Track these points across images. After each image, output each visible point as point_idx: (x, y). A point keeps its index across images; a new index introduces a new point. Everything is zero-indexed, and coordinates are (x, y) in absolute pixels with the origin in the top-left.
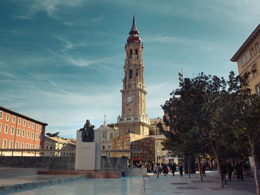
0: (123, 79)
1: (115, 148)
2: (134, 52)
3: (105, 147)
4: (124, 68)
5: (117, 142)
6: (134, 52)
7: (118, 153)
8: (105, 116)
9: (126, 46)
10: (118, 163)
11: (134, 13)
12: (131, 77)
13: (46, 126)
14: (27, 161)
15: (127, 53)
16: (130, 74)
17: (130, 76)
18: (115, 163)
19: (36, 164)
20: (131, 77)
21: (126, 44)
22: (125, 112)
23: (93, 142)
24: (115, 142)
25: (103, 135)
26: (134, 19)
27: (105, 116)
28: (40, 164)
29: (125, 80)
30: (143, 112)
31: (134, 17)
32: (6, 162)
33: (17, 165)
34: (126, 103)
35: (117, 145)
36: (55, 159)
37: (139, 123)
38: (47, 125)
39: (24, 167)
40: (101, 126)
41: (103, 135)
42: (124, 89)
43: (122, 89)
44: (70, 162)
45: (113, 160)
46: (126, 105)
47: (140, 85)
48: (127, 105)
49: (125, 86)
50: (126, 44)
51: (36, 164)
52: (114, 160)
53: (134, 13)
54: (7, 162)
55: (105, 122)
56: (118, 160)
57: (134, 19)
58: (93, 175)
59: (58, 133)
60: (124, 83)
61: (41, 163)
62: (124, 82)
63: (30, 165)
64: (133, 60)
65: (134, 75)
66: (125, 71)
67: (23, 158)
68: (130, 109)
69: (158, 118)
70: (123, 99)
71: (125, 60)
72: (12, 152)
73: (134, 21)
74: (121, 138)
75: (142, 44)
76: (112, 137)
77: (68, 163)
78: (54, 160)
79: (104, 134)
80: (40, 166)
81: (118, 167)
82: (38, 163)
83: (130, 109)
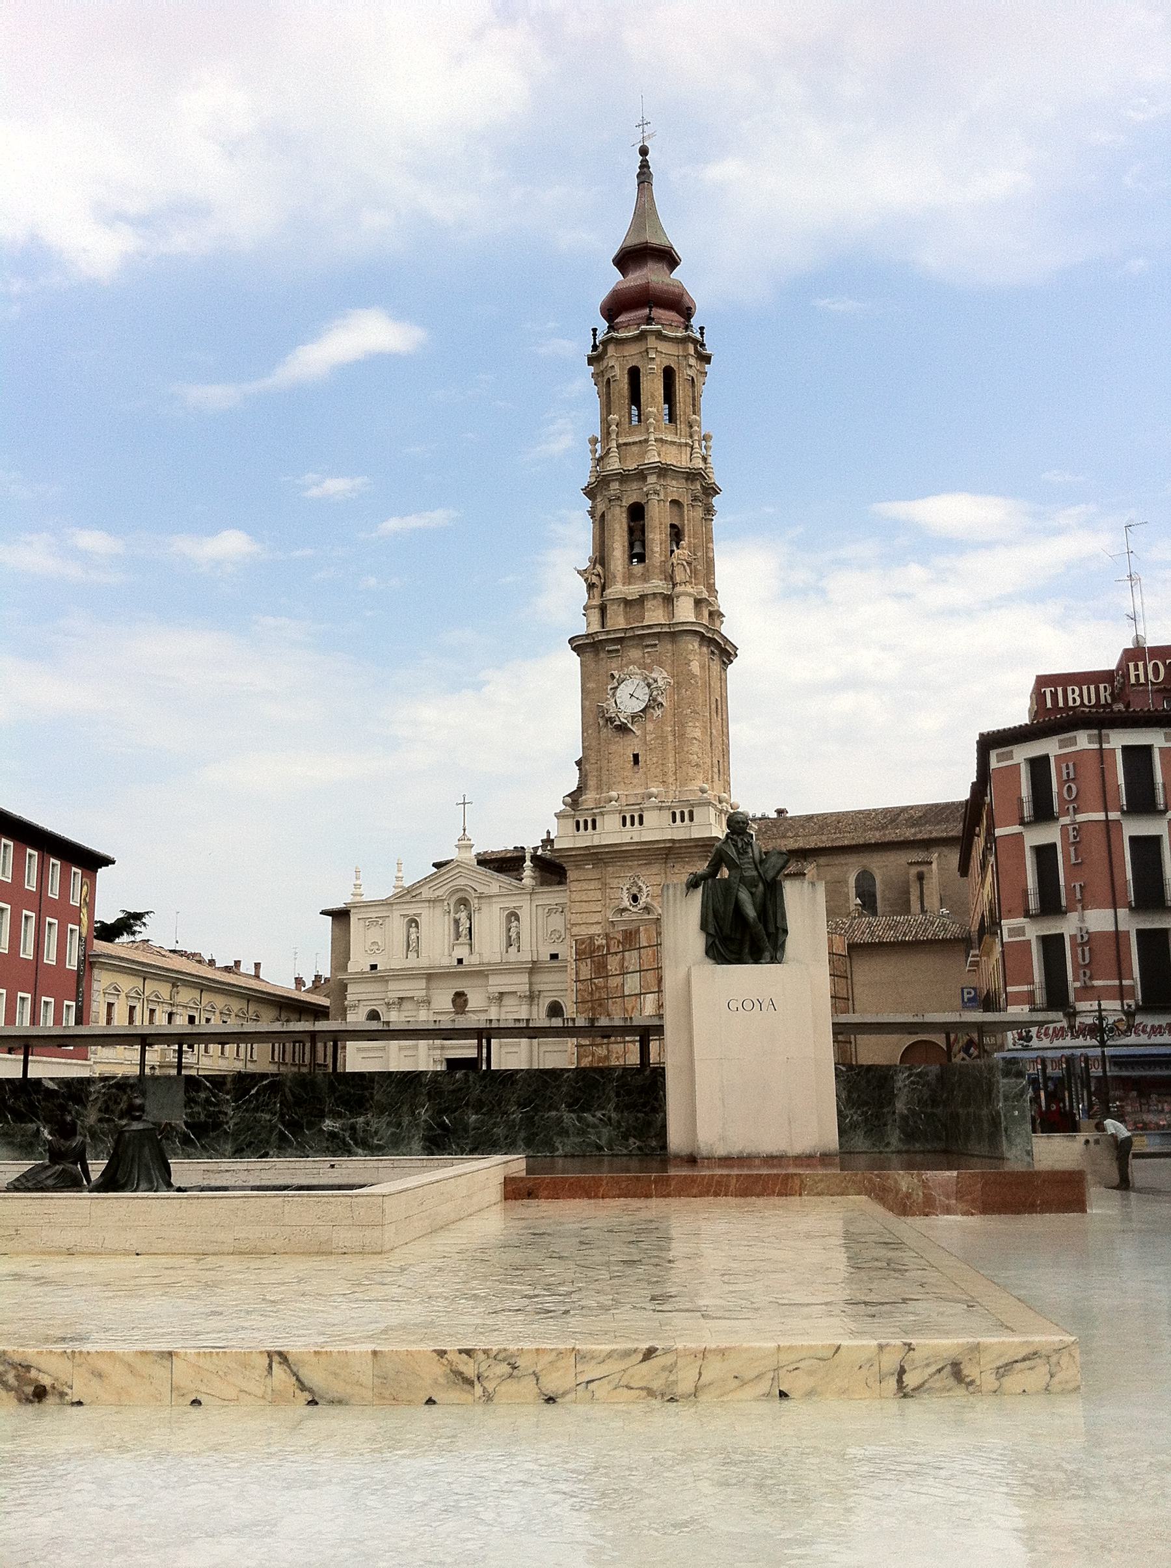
0: (586, 565)
1: (593, 1001)
2: (652, 386)
3: (466, 1001)
4: (590, 492)
5: (613, 964)
6: (652, 386)
7: (627, 1039)
8: (464, 804)
9: (595, 347)
10: (900, 1106)
11: (644, 124)
12: (637, 553)
13: (102, 872)
14: (256, 1109)
15: (608, 394)
16: (631, 531)
17: (631, 545)
18: (882, 1107)
19: (328, 1124)
20: (637, 553)
21: (595, 330)
22: (604, 778)
23: (775, 959)
24: (601, 968)
25: (457, 922)
26: (644, 165)
27: (464, 804)
28: (353, 1128)
29: (599, 568)
30: (716, 777)
31: (644, 151)
32: (100, 1120)
33: (186, 1141)
34: (610, 720)
35: (613, 982)
36: (460, 1089)
37: (702, 846)
38: (107, 861)
39: (238, 1152)
40: (436, 865)
41: (457, 922)
42: (596, 627)
43: (580, 627)
44: (569, 1106)
45: (863, 1082)
46: (607, 732)
47: (698, 602)
48: (623, 729)
49: (603, 609)
50: (595, 330)
51: (328, 1124)
52: (868, 1082)
53: (644, 124)
54: (109, 1120)
55: (464, 844)
56: (899, 1084)
57: (644, 165)
58: (908, 1196)
59: (138, 916)
60: (597, 591)
61: (361, 1119)
62: (591, 586)
63: (282, 1137)
64: (646, 441)
65: (657, 538)
66: (592, 514)
67: (229, 1086)
68: (636, 757)
69: (775, 815)
70: (585, 691)
71: (594, 441)
72: (139, 1047)
73: (644, 174)
74: (649, 939)
75: (702, 334)
76: (514, 936)
77: (554, 1113)
78: (453, 1091)
79: (463, 916)
80: (356, 1144)
81: (903, 1131)
82: (340, 1115)
83: (636, 757)
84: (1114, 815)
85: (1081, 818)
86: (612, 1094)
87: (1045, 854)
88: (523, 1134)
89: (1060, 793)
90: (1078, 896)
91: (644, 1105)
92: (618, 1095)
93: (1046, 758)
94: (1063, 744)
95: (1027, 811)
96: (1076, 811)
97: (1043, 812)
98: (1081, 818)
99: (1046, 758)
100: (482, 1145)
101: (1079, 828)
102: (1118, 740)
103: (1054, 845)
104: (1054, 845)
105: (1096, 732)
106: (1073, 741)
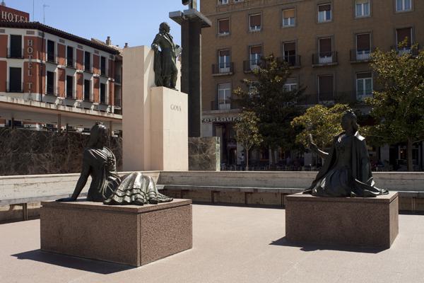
44: (34, 149)
84: (44, 62)
85: (33, 60)
86: (51, 145)
87: (15, 72)
88: (13, 164)
89: (24, 50)
90: (30, 87)
91: (63, 150)
92: (53, 145)
93: (20, 36)
94: (28, 33)
95: (9, 54)
96: (32, 58)
97: (16, 54)
98: (33, 60)
99: (20, 36)
100: (71, 170)
101: (34, 64)
102: (48, 37)
103: (20, 69)
104: (20, 69)
105: (41, 32)
106: (33, 33)
